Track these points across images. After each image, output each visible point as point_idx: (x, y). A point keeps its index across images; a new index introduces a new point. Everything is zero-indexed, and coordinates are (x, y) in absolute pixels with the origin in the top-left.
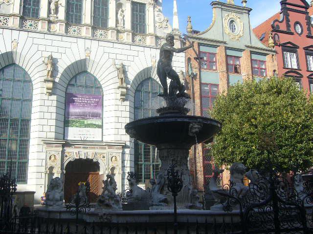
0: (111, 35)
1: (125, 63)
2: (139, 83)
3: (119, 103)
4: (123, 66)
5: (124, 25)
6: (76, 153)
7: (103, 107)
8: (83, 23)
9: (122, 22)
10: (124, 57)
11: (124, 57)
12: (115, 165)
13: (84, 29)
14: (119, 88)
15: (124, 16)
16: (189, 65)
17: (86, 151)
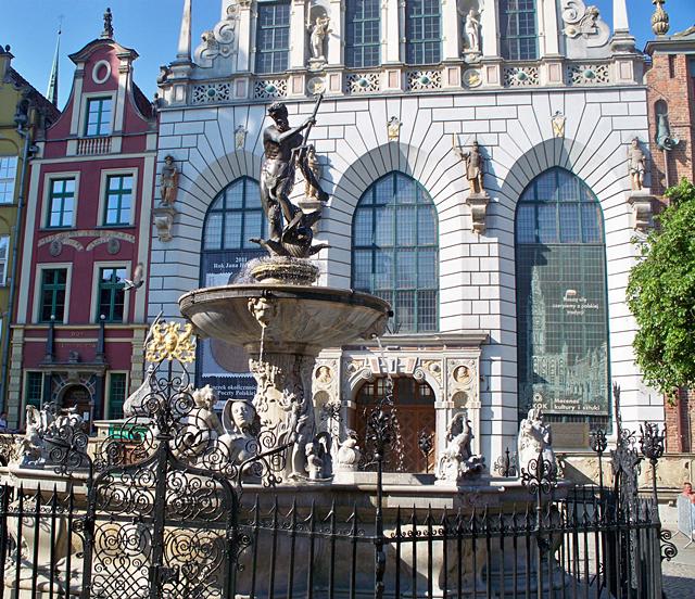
0: (449, 79)
1: (484, 140)
2: (526, 183)
3: (474, 237)
4: (479, 148)
5: (480, 48)
6: (373, 361)
7: (516, 246)
8: (383, 61)
9: (476, 42)
10: (484, 126)
11: (484, 126)
12: (463, 389)
13: (384, 77)
14: (470, 201)
15: (480, 28)
16: (661, 122)
17: (394, 356)
